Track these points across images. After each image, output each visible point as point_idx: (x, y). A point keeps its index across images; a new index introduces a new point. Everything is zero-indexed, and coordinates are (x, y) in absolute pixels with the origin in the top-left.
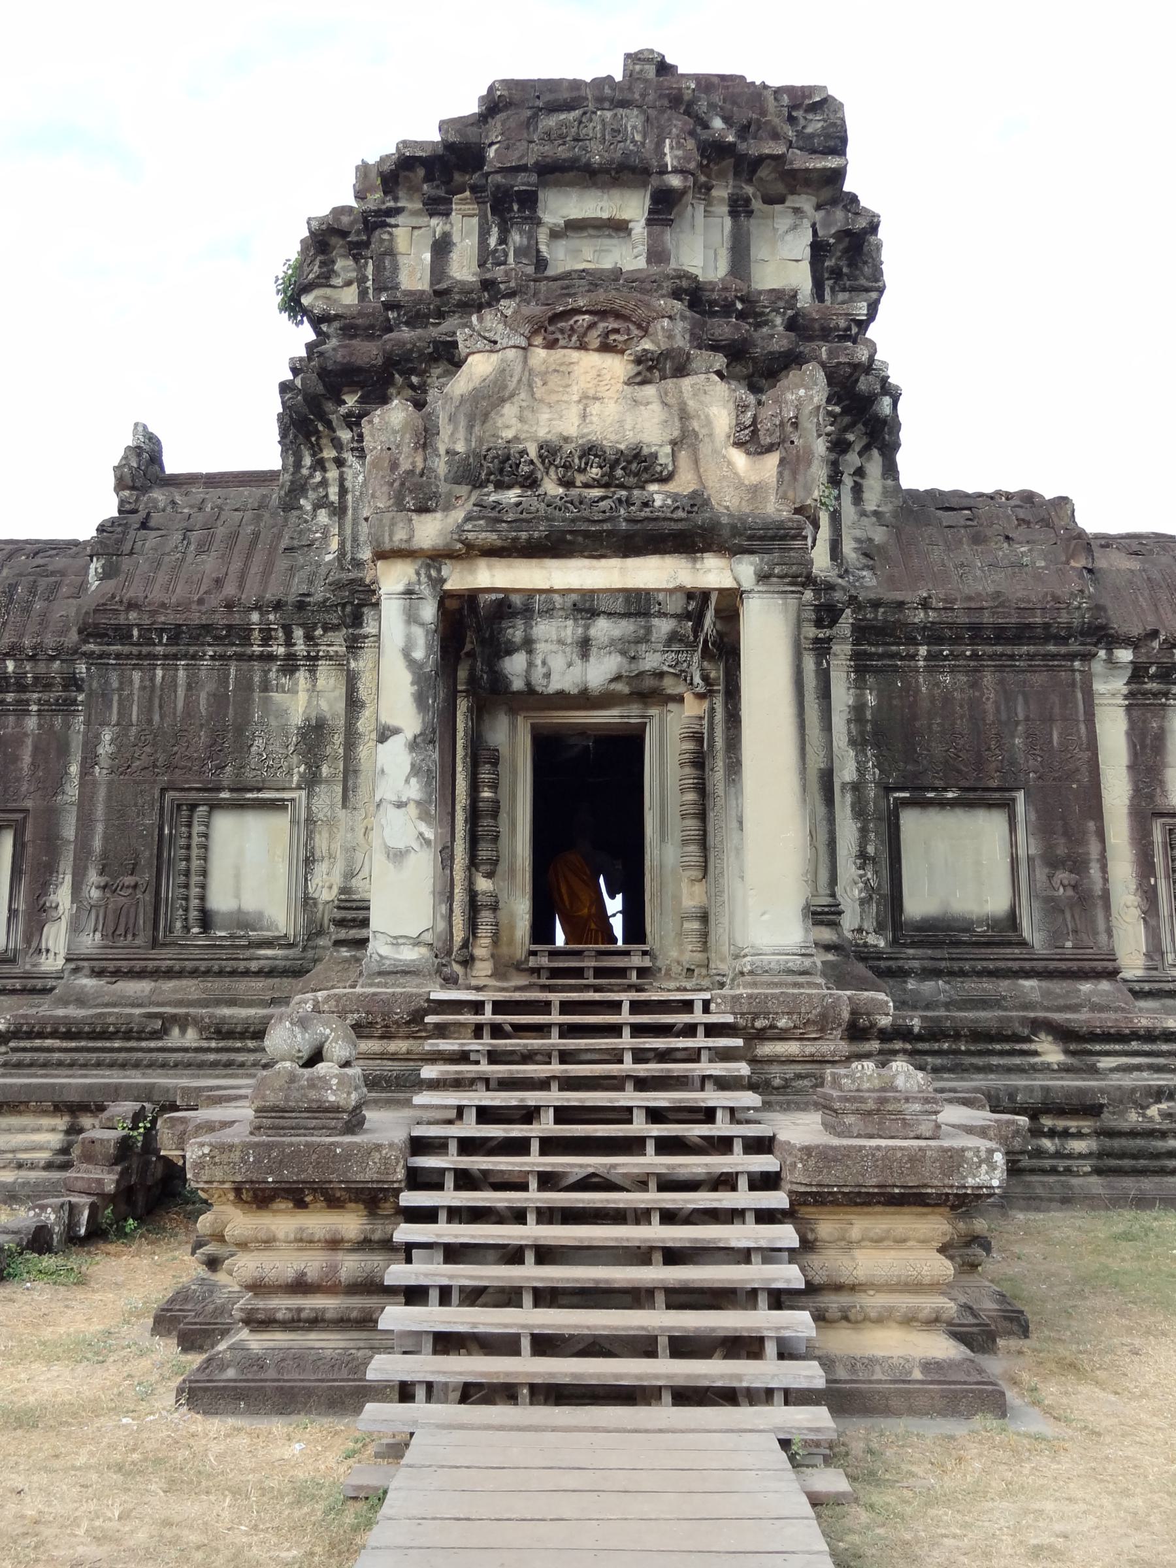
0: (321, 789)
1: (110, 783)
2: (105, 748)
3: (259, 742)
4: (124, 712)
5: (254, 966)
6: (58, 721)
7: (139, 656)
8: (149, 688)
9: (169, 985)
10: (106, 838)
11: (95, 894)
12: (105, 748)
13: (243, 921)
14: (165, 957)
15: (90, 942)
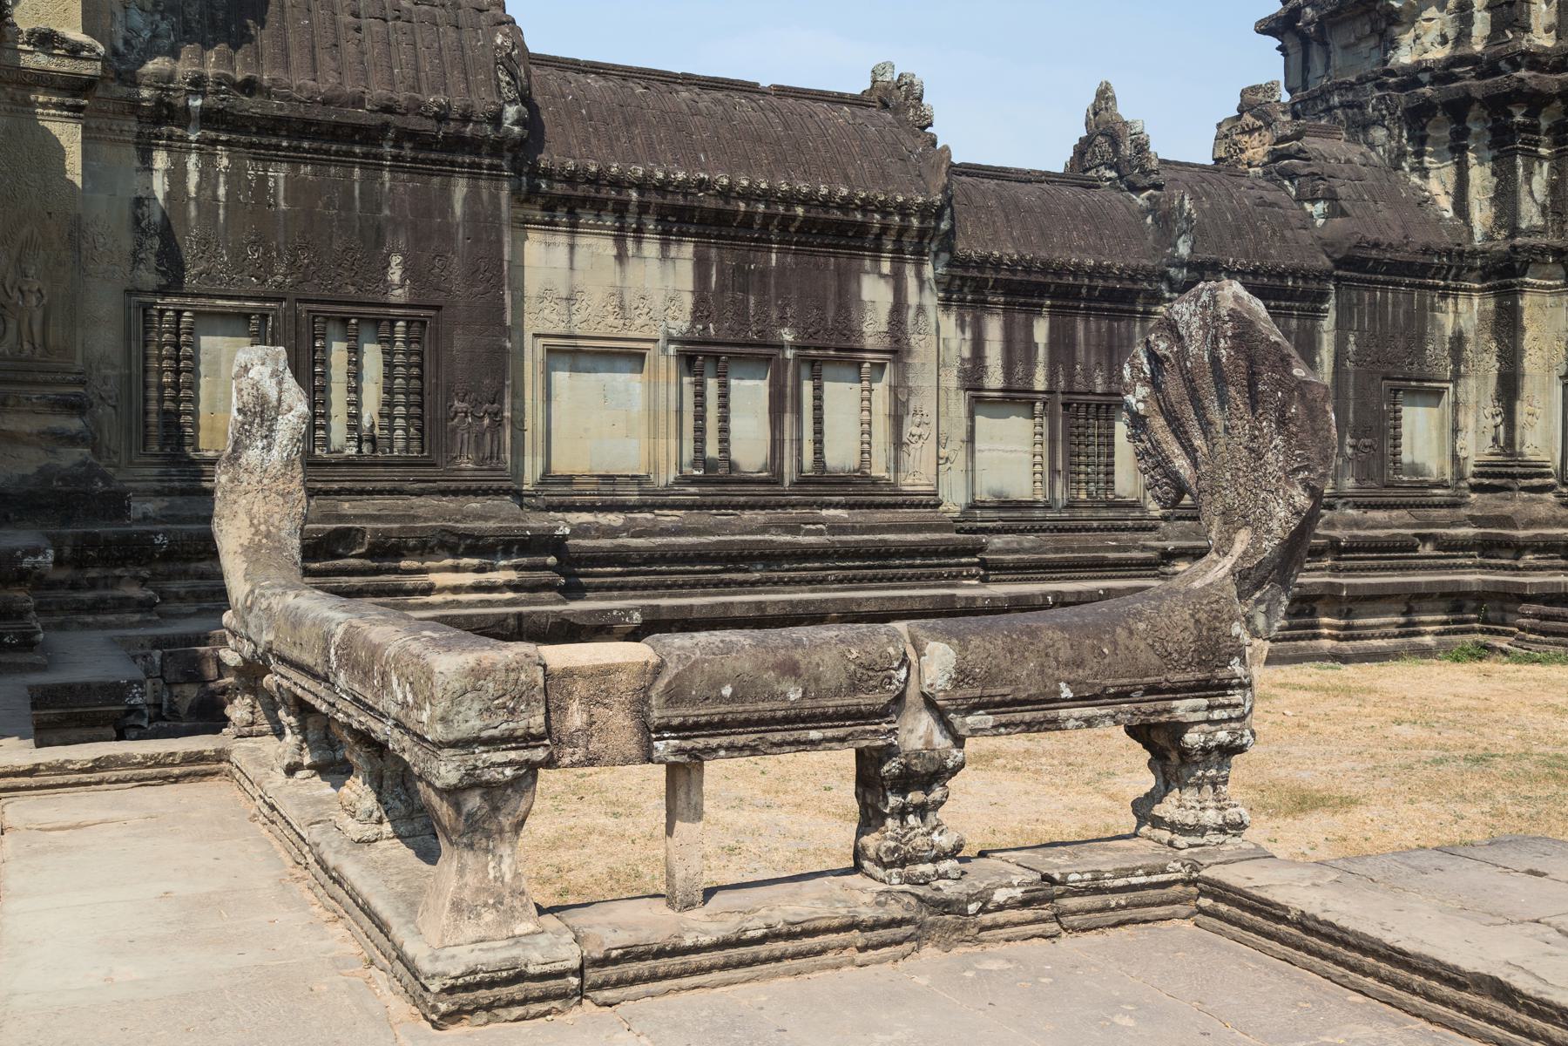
0: (1461, 381)
1: (1356, 373)
2: (1352, 347)
3: (1430, 347)
4: (1361, 322)
5: (1436, 499)
6: (1308, 323)
7: (1370, 282)
8: (1373, 303)
9: (1395, 513)
10: (1355, 413)
11: (1349, 451)
12: (1352, 347)
13: (1415, 469)
14: (1391, 496)
15: (1349, 483)
